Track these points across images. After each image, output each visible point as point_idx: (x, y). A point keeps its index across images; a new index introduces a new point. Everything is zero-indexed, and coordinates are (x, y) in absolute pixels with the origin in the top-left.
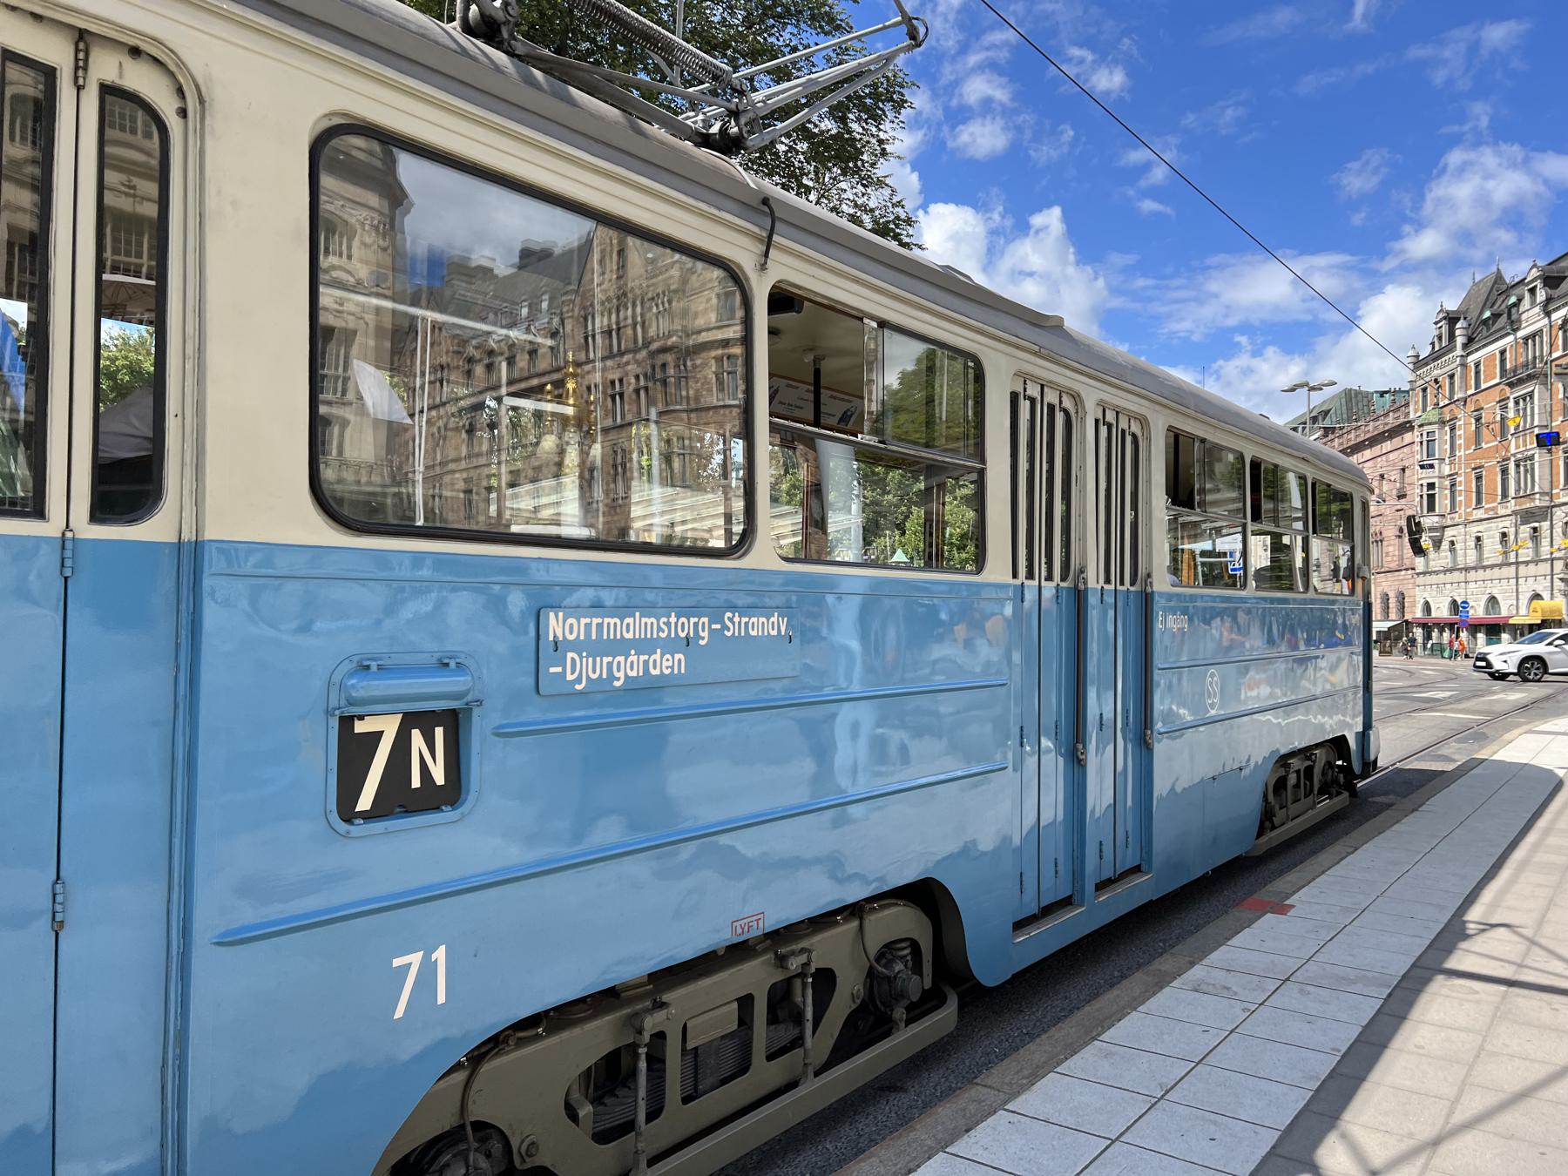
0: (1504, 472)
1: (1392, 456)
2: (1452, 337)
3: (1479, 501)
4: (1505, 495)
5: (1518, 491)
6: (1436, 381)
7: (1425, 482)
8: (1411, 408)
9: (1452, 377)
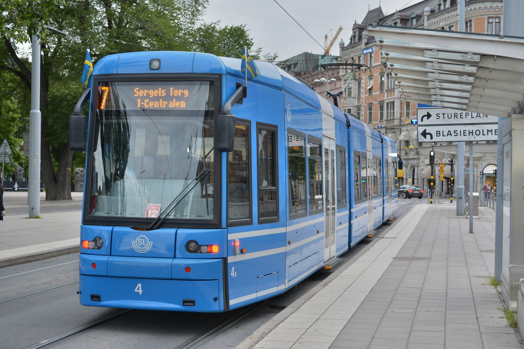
0: (382, 108)
2: (360, 38)
3: (370, 120)
4: (382, 118)
5: (387, 117)
6: (352, 58)
7: (347, 108)
9: (359, 58)
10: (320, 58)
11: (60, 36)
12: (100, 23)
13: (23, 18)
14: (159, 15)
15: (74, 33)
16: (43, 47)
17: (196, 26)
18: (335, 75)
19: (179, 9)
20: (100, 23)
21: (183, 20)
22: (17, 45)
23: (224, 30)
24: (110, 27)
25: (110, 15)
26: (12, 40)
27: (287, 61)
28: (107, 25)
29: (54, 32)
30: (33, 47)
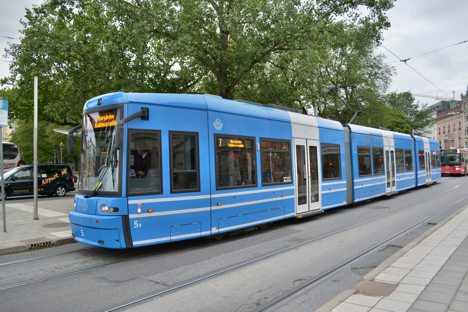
1: (457, 119)
8: (462, 107)
10: (450, 103)
11: (325, 104)
12: (343, 97)
13: (309, 98)
14: (369, 90)
15: (332, 102)
16: (318, 109)
17: (387, 93)
18: (459, 110)
19: (378, 87)
20: (343, 97)
21: (380, 92)
22: (307, 109)
23: (401, 94)
24: (347, 98)
25: (347, 93)
26: (305, 107)
27: (433, 106)
28: (345, 97)
29: (323, 103)
30: (314, 109)
